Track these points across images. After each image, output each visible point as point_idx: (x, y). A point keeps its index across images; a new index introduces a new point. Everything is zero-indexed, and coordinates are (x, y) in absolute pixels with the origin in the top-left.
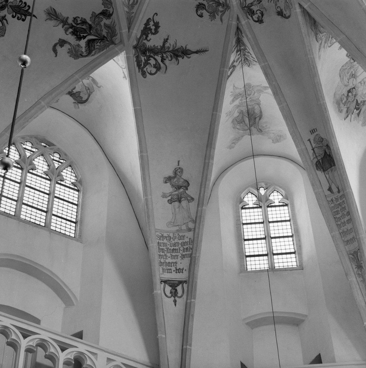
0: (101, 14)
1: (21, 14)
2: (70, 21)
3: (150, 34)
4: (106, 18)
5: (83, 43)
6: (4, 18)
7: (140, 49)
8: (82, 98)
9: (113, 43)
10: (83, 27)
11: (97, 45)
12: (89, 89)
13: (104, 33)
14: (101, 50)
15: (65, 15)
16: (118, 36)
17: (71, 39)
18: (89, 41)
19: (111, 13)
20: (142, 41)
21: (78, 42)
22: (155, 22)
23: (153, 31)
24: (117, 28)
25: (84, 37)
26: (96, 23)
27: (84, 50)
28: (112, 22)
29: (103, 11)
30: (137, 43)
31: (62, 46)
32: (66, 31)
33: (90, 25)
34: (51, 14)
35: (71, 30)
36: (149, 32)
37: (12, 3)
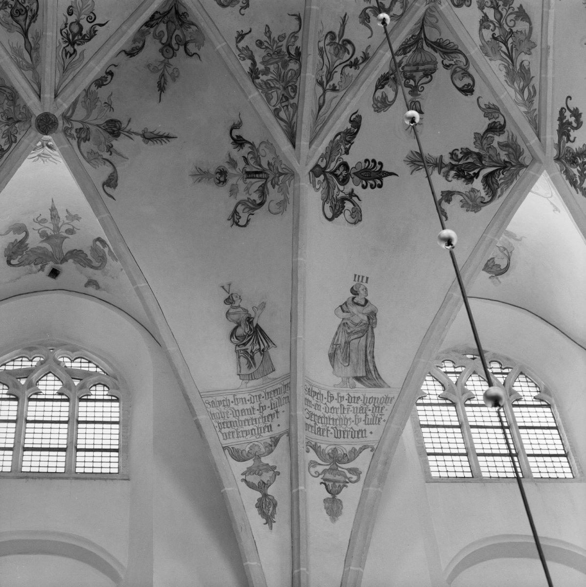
0: (487, 131)
1: (373, 179)
2: (447, 160)
3: (572, 131)
4: (498, 134)
5: (478, 184)
6: (352, 194)
7: (566, 159)
8: (499, 266)
9: (522, 166)
10: (469, 161)
11: (501, 178)
12: (505, 249)
13: (503, 157)
14: (508, 183)
15: (436, 155)
16: (526, 153)
17: (458, 185)
18: (486, 178)
19: (502, 123)
20: (564, 147)
21: (470, 186)
22: (572, 109)
23: (575, 125)
24: (520, 142)
25: (477, 175)
26: (485, 149)
27: (483, 194)
28: (508, 136)
29: (489, 126)
30: (558, 151)
31: (449, 201)
32: (446, 176)
33: (478, 154)
34: (416, 161)
35: (452, 173)
36: (569, 128)
37: (355, 168)
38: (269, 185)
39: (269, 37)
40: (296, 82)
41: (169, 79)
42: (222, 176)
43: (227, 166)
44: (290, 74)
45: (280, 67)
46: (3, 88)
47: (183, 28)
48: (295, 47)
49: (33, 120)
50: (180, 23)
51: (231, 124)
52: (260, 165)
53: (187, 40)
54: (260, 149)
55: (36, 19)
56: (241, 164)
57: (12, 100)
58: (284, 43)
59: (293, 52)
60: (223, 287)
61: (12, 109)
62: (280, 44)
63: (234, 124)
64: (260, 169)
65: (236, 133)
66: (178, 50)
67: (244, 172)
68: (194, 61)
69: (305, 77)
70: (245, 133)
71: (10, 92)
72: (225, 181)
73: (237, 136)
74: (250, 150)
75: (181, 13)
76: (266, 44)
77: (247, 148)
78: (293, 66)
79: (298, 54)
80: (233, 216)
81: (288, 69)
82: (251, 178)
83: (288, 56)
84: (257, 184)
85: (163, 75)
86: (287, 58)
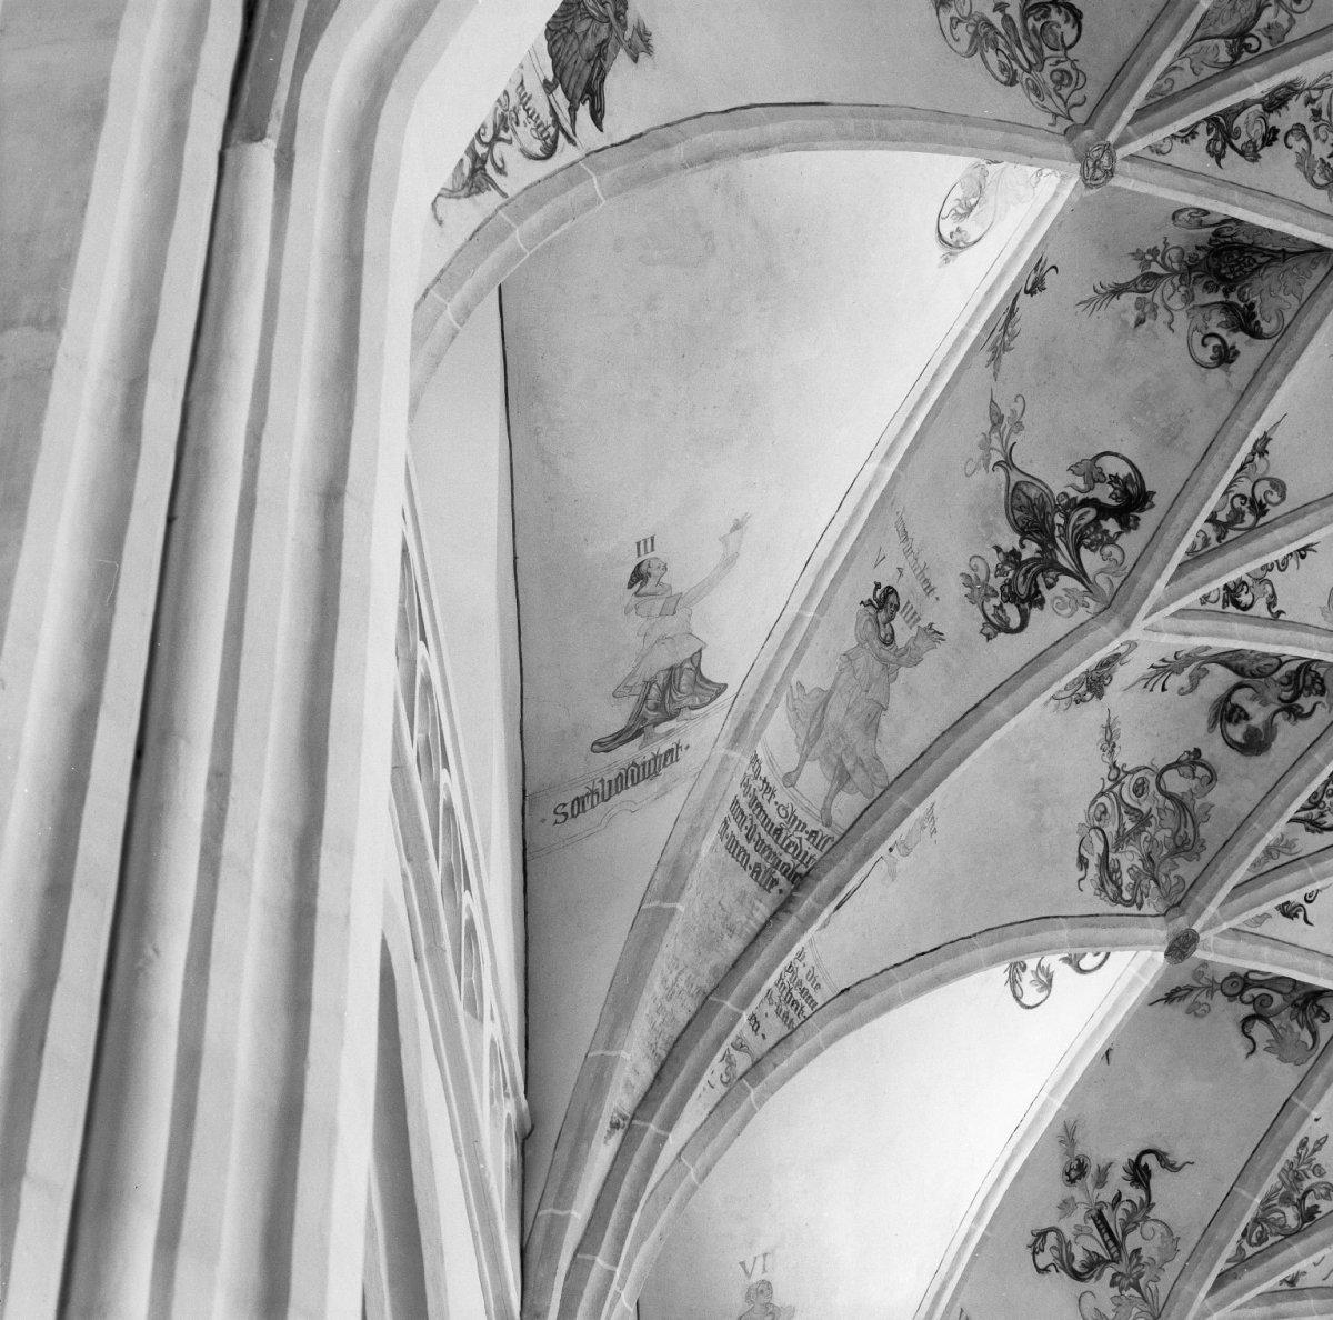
38: (1109, 1272)
39: (1314, 1151)
40: (1272, 1234)
41: (1189, 1001)
42: (1076, 1171)
43: (1092, 1170)
44: (1276, 1215)
45: (1281, 1192)
46: (1189, 817)
47: (1291, 1009)
48: (1316, 1202)
49: (1181, 923)
50: (1299, 1002)
51: (1164, 1148)
52: (1125, 1234)
53: (1271, 1019)
54: (1149, 1225)
55: (1313, 832)
56: (1107, 1195)
57: (1177, 847)
58: (1314, 1180)
59: (1308, 1203)
60: (962, 1310)
61: (1165, 853)
62: (1310, 1173)
63: (1165, 1154)
64: (1119, 1237)
65: (1150, 1160)
66: (1243, 1002)
67: (1098, 1207)
68: (1239, 1044)
69: (1290, 1246)
70: (1160, 1180)
71: (1191, 836)
72: (1072, 1181)
73: (1146, 1165)
74: (1137, 1202)
75: (1321, 1002)
76: (1304, 1152)
77: (1136, 1194)
78: (1291, 1216)
79: (1309, 1216)
80: (1039, 1235)
81: (1283, 1208)
82: (1097, 1226)
83: (1299, 1196)
84: (1095, 1244)
85: (1191, 989)
86: (1296, 1196)
